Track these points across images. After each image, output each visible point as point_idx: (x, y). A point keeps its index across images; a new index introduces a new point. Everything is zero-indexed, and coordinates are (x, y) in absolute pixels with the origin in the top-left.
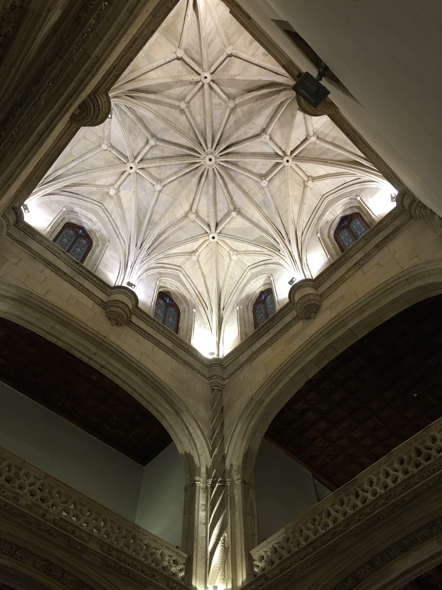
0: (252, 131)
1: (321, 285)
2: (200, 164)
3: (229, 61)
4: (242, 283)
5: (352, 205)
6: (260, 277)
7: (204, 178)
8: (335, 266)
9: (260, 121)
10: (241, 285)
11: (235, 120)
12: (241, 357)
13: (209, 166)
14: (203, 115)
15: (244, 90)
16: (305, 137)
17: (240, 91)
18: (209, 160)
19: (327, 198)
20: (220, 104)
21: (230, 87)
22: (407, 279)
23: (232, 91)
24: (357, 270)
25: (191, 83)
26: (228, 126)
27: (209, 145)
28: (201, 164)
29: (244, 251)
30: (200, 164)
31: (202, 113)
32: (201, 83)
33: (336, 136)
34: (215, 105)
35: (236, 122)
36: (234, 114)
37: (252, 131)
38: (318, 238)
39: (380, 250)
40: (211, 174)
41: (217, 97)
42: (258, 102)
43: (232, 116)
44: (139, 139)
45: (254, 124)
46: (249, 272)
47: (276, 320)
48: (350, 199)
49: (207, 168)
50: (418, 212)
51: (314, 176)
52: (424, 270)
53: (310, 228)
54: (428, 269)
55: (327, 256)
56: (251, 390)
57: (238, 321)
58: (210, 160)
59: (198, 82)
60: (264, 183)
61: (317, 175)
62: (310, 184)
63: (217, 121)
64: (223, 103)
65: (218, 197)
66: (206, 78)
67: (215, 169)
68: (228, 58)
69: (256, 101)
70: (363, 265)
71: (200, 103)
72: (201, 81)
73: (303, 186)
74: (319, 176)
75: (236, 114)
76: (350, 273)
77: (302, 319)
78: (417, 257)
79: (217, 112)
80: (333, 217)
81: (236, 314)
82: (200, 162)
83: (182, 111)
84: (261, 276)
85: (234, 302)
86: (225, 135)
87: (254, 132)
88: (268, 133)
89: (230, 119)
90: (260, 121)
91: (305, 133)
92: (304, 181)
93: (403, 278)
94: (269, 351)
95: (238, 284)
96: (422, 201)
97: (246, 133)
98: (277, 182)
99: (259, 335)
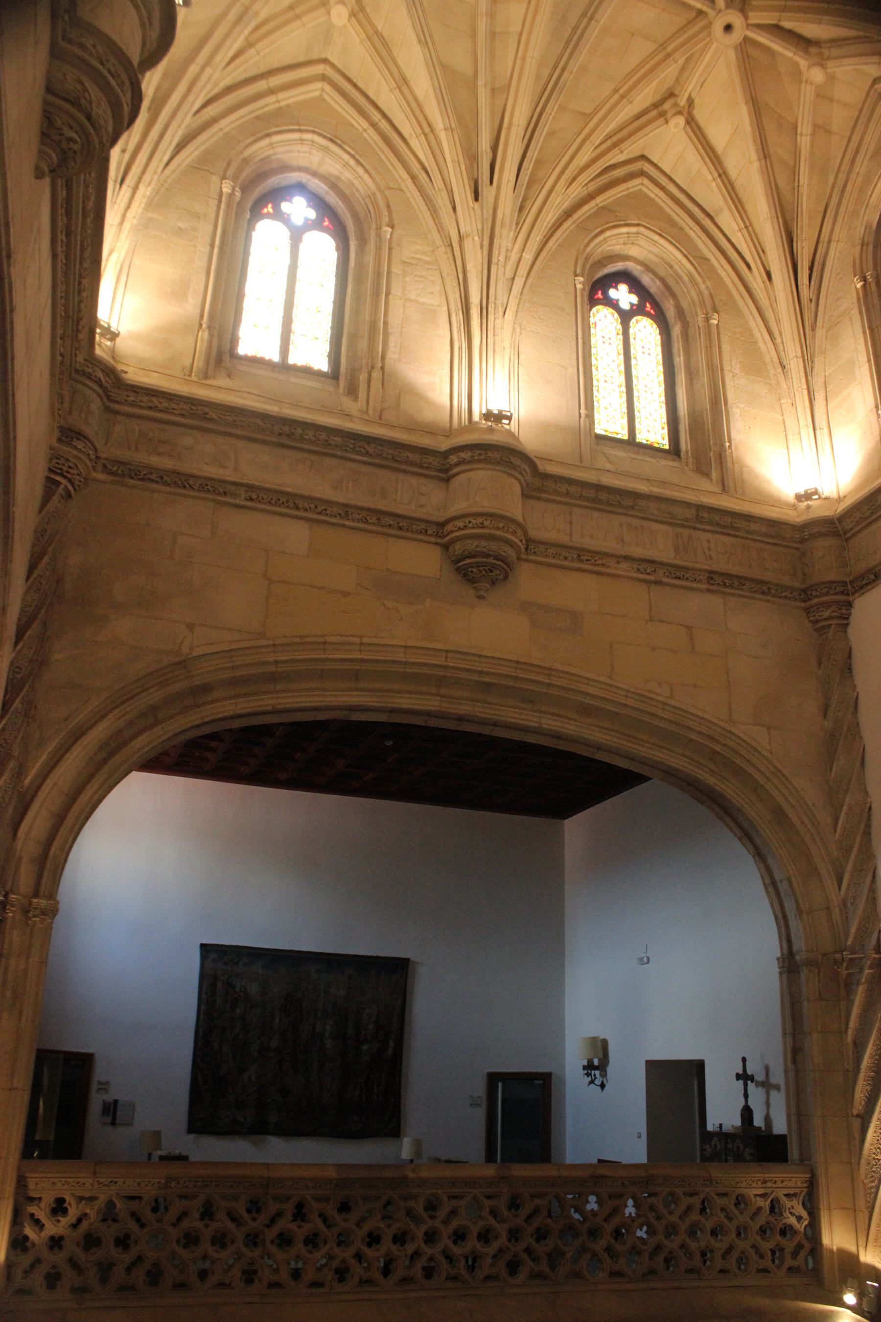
1: (539, 499)
4: (281, 96)
5: (671, 282)
6: (346, 157)
8: (603, 496)
10: (272, 99)
12: (188, 441)
19: (646, 181)
22: (715, 752)
24: (641, 580)
29: (377, 33)
38: (572, 291)
39: (708, 590)
46: (319, 85)
50: (826, 614)
51: (696, 113)
52: (762, 781)
53: (569, 222)
54: (768, 786)
55: (580, 408)
56: (191, 627)
57: (212, 246)
61: (702, 123)
70: (658, 583)
73: (658, 97)
74: (700, 128)
77: (446, 547)
78: (769, 728)
80: (616, 247)
81: (213, 203)
84: (352, 162)
85: (221, 134)
92: (671, 94)
93: (717, 748)
94: (295, 535)
95: (262, 85)
96: (853, 611)
99: (289, 436)
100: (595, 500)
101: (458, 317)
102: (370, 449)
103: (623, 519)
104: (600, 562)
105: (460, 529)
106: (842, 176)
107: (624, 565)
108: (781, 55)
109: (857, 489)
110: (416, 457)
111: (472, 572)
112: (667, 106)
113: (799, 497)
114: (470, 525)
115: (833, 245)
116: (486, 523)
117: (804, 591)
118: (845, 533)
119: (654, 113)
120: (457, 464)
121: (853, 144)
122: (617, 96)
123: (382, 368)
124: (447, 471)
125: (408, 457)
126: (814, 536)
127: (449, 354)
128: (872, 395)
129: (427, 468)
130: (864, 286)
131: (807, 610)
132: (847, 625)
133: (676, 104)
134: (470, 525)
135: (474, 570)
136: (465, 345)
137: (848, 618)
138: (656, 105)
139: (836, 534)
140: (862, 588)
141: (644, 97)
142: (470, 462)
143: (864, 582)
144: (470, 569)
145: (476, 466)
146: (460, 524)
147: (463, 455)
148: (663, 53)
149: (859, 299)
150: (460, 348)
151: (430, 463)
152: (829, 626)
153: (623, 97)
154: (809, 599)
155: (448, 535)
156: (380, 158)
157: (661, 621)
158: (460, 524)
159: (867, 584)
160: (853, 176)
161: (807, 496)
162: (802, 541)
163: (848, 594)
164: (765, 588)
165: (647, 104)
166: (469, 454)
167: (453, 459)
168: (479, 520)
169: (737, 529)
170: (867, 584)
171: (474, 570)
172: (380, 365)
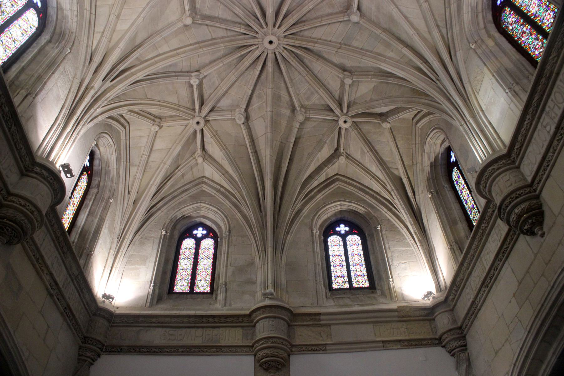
0: (257, 105)
2: (277, 25)
3: (334, 146)
7: (259, 15)
9: (260, 127)
11: (282, 99)
13: (266, 34)
14: (316, 72)
15: (300, 138)
16: (206, 147)
17: (303, 133)
18: (271, 40)
19: (124, 132)
20: (308, 99)
21: (314, 127)
23: (309, 126)
25: (355, 103)
26: (283, 85)
27: (285, 54)
28: (276, 27)
30: (277, 25)
31: (319, 75)
32: (345, 111)
33: (185, 177)
34: (312, 93)
35: (280, 97)
36: (287, 103)
37: (257, 105)
39: (62, 314)
40: (256, 27)
41: (317, 102)
42: (279, 143)
43: (287, 98)
44: (373, 8)
45: (261, 117)
47: (9, 129)
48: (113, 177)
49: (265, 29)
50: (89, 354)
58: (271, 42)
59: (349, 106)
60: (195, 82)
62: (155, 129)
63: (297, 79)
64: (307, 103)
65: (222, 6)
66: (345, 122)
67: (257, 36)
68: (336, 147)
69: (281, 142)
70: (51, 295)
71: (329, 84)
72: (346, 114)
73: (157, 115)
75: (286, 105)
76: (47, 278)
79: (304, 88)
82: (279, 28)
83: (344, 69)
86: (277, 74)
87: (254, 106)
88: (242, 125)
89: (287, 94)
90: (260, 127)
91: (210, 153)
92: (160, 118)
96: (99, 359)
97: (260, 97)
98: (184, 92)
100: (57, 238)
101: (65, 112)
102: (13, 128)
103: (58, 256)
104: (43, 268)
105: (21, 205)
106: (176, 194)
107: (48, 277)
108: (196, 143)
109: (126, 308)
110: (23, 151)
111: (7, 230)
112: (157, 120)
113: (104, 296)
114: (28, 207)
115: (160, 212)
116: (35, 213)
117: (85, 337)
118: (113, 323)
119: (153, 118)
120: (37, 173)
121: (186, 188)
122: (158, 103)
123: (34, 98)
124: (27, 170)
125: (22, 149)
126: (100, 315)
127: (53, 122)
128: (151, 276)
129: (22, 161)
130: (165, 235)
131: (80, 347)
132: (92, 364)
133: (160, 123)
134: (28, 207)
135: (10, 229)
136: (62, 125)
137: (94, 361)
138: (156, 117)
139: (109, 321)
140: (110, 352)
141: (155, 111)
142: (44, 178)
143: (113, 350)
144: (7, 228)
145: (46, 183)
146: (23, 202)
147: (44, 172)
148: (178, 107)
149: (161, 238)
150: (59, 125)
151: (25, 160)
152: (86, 361)
153: (159, 105)
154: (85, 343)
155: (9, 201)
156: (82, 25)
157: (43, 315)
158: (23, 202)
159: (113, 351)
160: (180, 197)
161: (107, 297)
162: (95, 315)
163: (102, 351)
164: (77, 327)
165: (154, 113)
166: (47, 174)
167: (38, 169)
168: (33, 209)
169: (82, 292)
170: (113, 351)
171: (10, 229)
172: (34, 96)
